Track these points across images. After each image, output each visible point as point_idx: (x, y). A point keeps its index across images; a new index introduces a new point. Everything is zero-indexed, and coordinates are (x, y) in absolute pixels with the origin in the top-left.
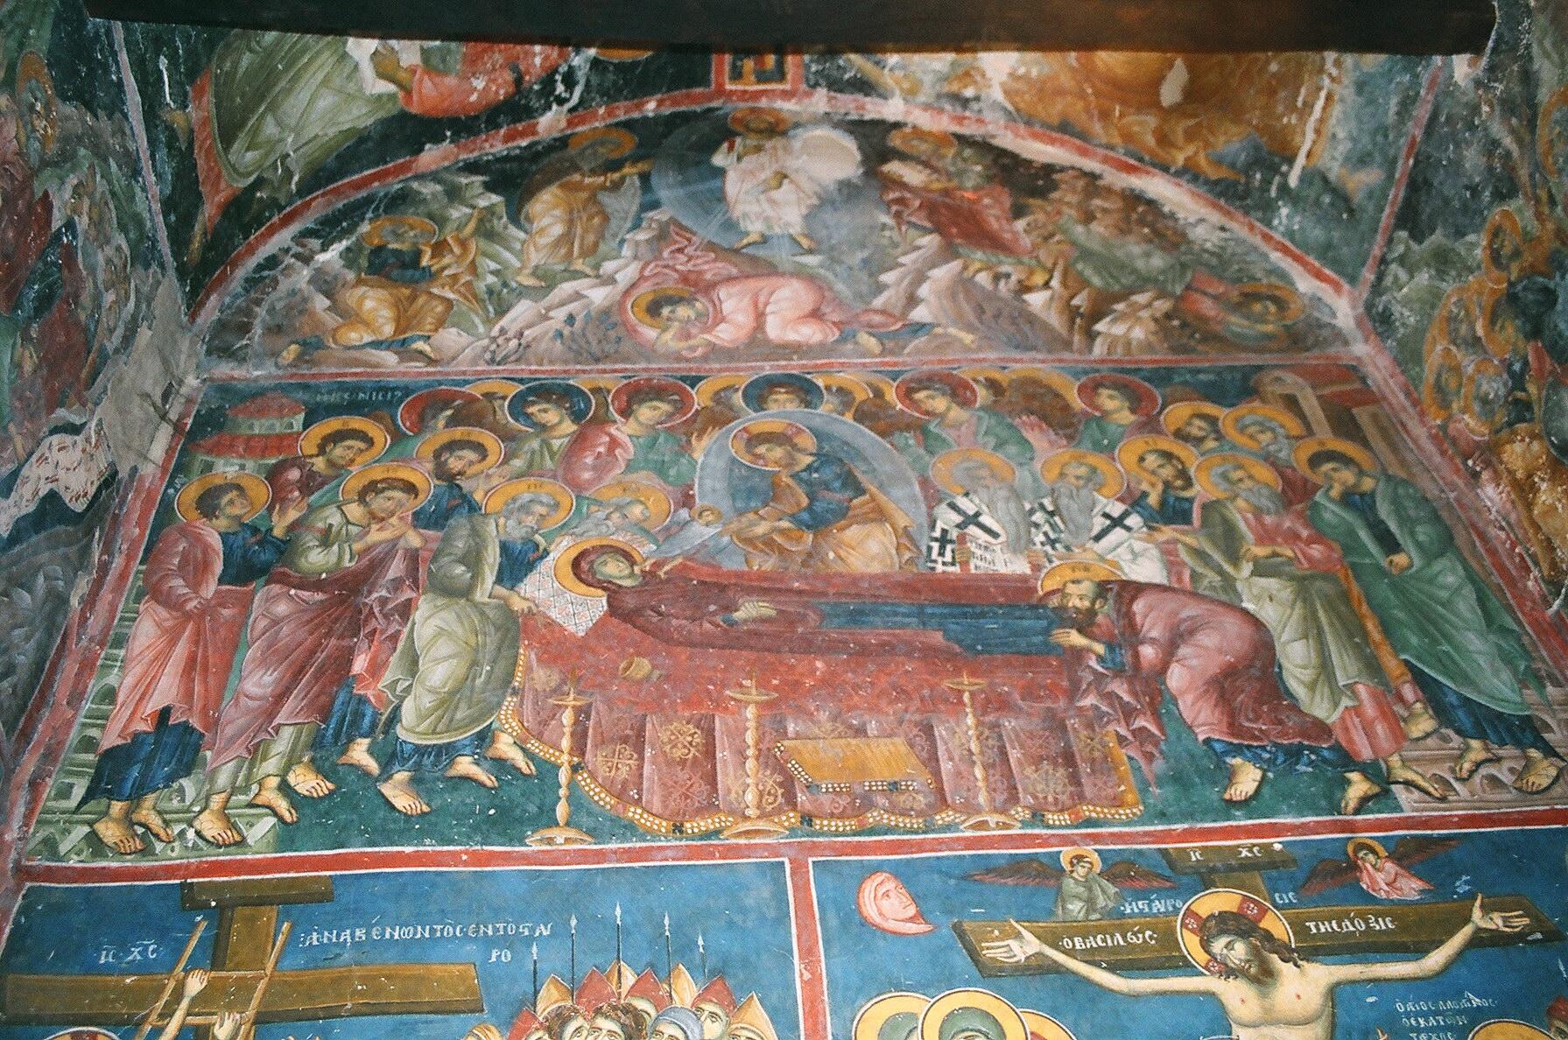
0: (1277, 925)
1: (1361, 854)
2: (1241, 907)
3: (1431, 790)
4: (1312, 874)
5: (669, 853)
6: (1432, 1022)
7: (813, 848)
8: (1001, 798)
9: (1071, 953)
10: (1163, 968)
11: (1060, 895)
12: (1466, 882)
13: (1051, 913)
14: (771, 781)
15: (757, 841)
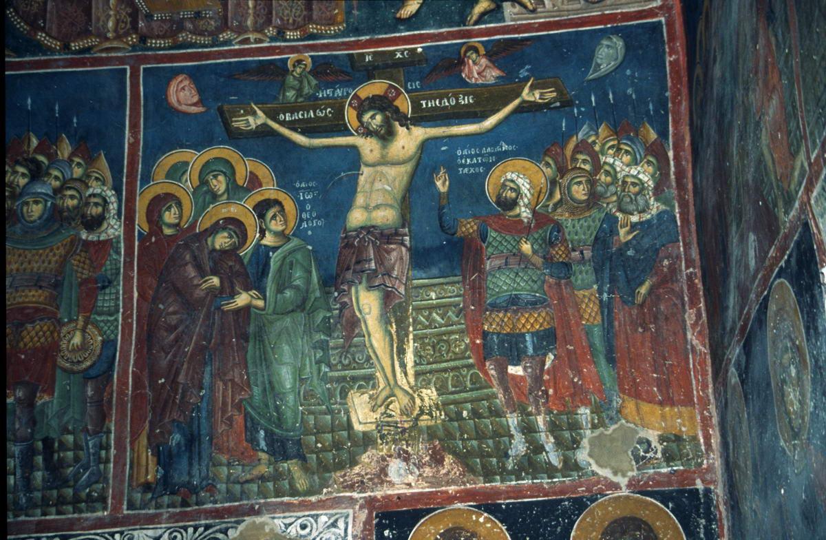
0: (405, 104)
1: (468, 54)
2: (386, 92)
3: (529, 4)
4: (434, 69)
5: (61, 63)
6: (475, 161)
7: (145, 59)
8: (261, 21)
9: (283, 123)
10: (333, 131)
11: (283, 87)
12: (527, 70)
13: (276, 98)
14: (125, 12)
15: (113, 54)
